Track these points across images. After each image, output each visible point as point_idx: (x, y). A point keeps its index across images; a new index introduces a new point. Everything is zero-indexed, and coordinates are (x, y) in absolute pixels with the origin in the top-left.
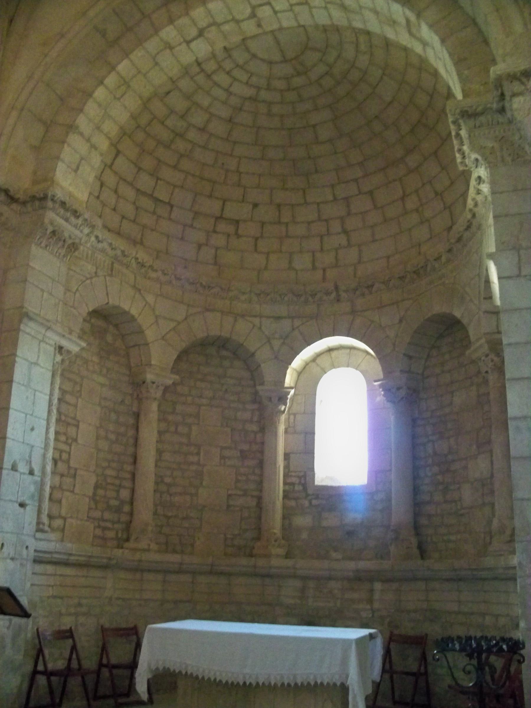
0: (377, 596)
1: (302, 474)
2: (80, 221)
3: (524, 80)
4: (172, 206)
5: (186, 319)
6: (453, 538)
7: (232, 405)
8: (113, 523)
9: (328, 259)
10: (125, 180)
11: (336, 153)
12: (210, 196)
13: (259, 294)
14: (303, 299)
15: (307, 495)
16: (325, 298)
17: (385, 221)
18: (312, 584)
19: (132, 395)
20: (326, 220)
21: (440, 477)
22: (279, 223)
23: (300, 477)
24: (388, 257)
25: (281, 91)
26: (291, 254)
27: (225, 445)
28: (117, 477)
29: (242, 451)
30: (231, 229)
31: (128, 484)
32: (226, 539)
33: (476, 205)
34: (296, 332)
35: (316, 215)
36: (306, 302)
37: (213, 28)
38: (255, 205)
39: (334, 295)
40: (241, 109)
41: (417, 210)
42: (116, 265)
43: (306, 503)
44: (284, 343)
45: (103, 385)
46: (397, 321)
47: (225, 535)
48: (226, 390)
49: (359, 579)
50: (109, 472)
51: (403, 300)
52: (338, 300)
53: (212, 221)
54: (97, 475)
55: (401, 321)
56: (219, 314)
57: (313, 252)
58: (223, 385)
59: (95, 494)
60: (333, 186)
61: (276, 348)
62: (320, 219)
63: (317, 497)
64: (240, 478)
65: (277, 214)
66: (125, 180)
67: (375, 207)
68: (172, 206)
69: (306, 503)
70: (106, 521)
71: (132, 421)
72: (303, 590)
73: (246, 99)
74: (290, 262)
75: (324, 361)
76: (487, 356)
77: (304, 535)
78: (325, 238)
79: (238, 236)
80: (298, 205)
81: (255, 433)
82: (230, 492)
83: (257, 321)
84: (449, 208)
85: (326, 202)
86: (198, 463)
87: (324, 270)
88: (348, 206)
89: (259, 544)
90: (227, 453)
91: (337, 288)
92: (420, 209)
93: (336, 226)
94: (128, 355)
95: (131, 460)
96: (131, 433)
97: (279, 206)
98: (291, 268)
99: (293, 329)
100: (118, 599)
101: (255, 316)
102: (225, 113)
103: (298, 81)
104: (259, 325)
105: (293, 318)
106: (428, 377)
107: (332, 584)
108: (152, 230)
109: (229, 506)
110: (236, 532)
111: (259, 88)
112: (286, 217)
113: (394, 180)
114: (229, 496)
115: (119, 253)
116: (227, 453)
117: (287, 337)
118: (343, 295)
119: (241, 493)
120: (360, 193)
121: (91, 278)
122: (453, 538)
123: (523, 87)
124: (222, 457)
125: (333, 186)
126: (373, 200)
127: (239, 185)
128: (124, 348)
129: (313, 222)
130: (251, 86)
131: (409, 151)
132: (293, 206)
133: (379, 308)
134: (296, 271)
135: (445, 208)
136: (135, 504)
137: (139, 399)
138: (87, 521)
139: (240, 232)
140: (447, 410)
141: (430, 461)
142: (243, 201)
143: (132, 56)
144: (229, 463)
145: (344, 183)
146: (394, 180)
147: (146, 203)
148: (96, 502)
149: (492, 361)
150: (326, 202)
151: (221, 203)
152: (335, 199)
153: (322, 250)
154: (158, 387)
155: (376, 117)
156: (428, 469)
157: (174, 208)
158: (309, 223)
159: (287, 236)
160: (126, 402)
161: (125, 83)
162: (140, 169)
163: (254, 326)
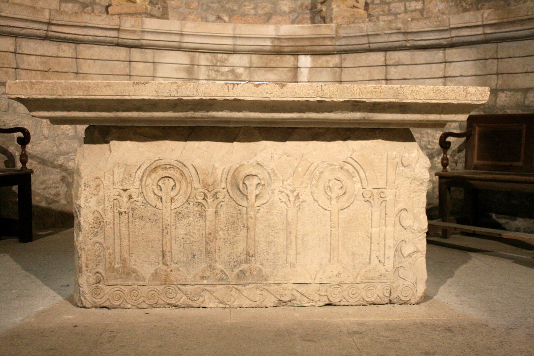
18: (203, 59)
49: (278, 52)
107: (235, 59)
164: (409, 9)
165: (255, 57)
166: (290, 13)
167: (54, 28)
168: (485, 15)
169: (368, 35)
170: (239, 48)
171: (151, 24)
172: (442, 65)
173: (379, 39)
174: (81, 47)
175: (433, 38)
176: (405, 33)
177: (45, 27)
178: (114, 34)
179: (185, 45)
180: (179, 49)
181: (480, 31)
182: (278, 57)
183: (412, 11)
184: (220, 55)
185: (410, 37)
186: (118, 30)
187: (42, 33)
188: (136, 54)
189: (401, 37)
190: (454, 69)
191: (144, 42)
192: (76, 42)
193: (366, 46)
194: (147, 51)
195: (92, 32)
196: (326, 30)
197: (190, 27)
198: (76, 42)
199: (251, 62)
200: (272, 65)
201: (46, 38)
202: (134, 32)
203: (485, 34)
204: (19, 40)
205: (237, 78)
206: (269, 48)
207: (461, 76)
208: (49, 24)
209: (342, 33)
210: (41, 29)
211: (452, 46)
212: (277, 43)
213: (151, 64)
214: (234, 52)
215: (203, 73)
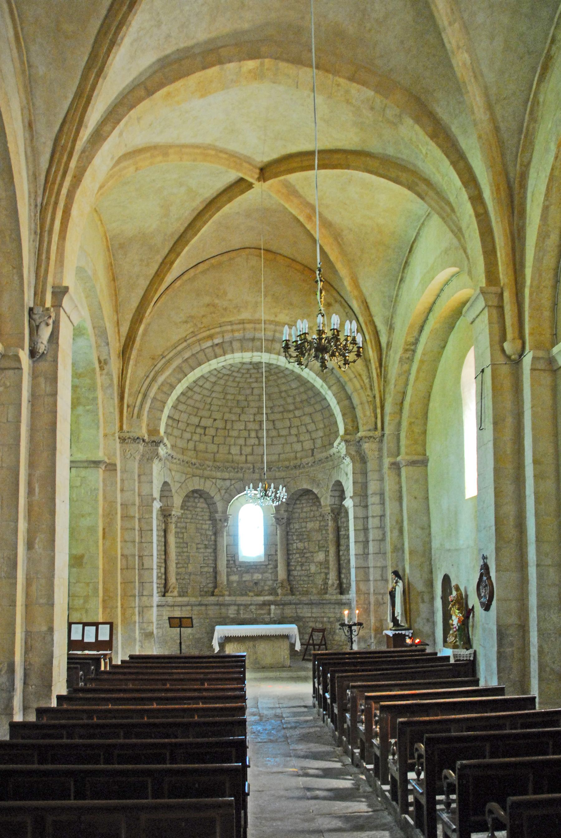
9: (248, 450)
20: (249, 430)
21: (300, 559)
22: (225, 429)
26: (230, 445)
30: (202, 431)
31: (163, 565)
34: (232, 487)
38: (215, 420)
41: (296, 435)
43: (235, 570)
52: (254, 472)
60: (255, 415)
62: (245, 429)
63: (240, 567)
67: (275, 428)
69: (235, 570)
77: (235, 585)
78: (247, 439)
83: (214, 481)
85: (250, 421)
87: (246, 456)
90: (199, 546)
93: (253, 434)
95: (163, 553)
96: (163, 540)
97: (226, 421)
98: (229, 453)
105: (231, 480)
109: (201, 572)
116: (199, 546)
118: (257, 471)
124: (197, 548)
126: (274, 425)
131: (296, 409)
132: (233, 421)
136: (168, 575)
137: (166, 523)
140: (304, 529)
150: (250, 421)
152: (254, 420)
153: (245, 445)
158: (240, 430)
159: (228, 436)
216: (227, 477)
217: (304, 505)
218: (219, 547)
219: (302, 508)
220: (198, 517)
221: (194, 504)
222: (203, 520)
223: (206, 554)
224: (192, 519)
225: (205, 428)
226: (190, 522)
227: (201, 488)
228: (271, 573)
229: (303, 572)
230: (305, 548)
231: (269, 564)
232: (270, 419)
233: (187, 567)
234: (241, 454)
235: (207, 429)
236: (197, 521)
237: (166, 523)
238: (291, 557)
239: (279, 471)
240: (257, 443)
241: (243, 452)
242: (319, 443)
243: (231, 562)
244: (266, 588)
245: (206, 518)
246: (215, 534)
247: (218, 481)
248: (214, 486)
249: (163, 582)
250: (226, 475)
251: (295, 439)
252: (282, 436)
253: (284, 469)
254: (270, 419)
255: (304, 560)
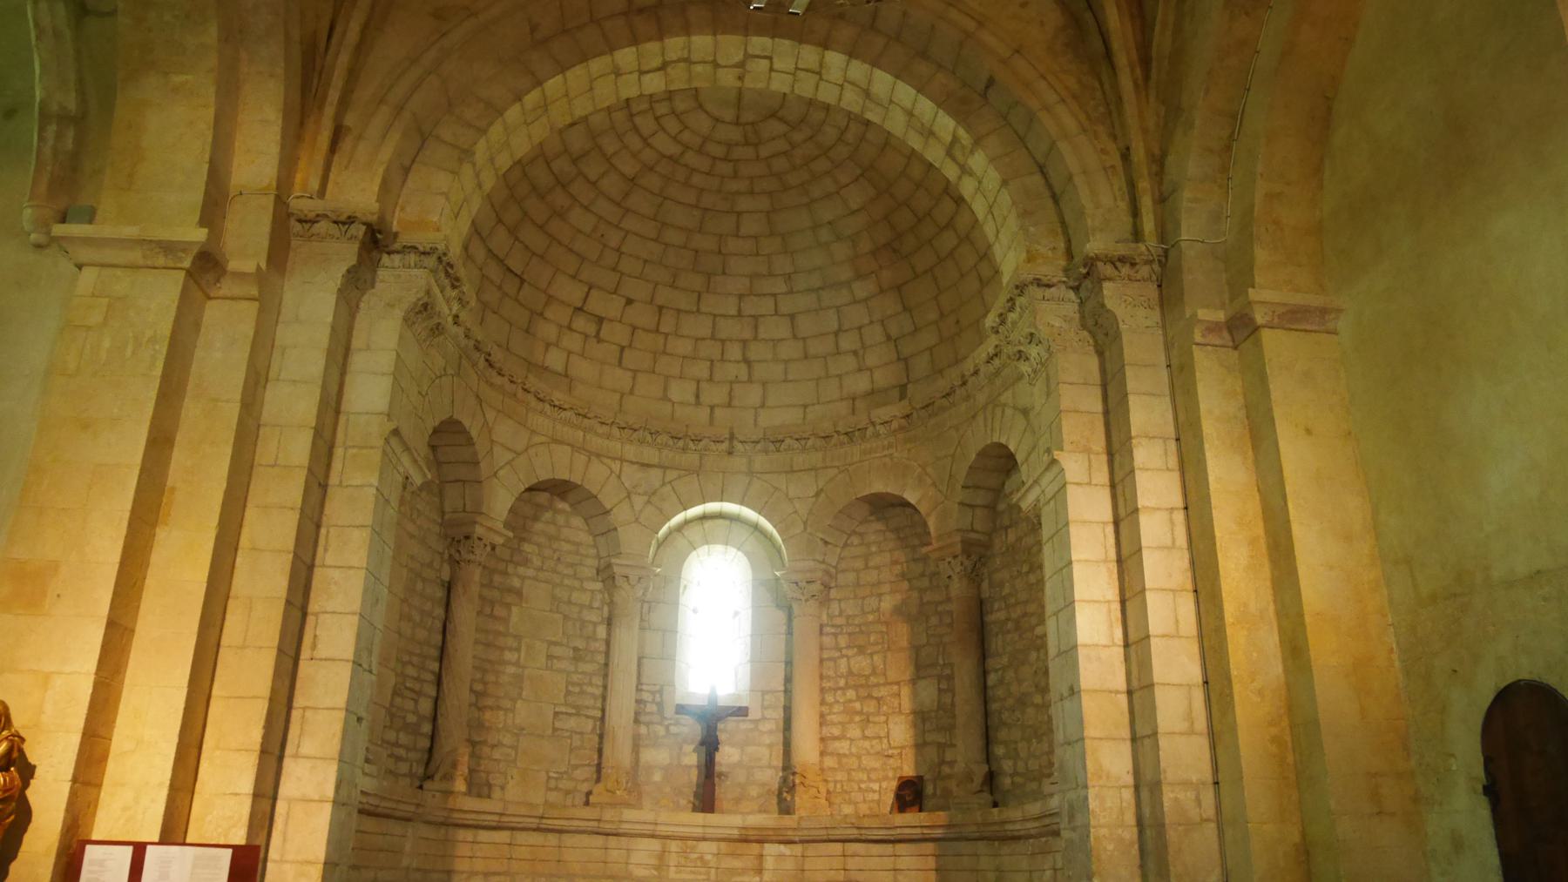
0: (769, 863)
1: (657, 688)
2: (454, 293)
3: (1118, 264)
4: (522, 281)
5: (526, 450)
6: (876, 786)
7: (566, 582)
8: (408, 749)
10: (479, 234)
11: (757, 254)
12: (574, 277)
13: (624, 428)
14: (681, 443)
15: (664, 718)
16: (713, 446)
17: (806, 357)
18: (674, 846)
19: (441, 554)
20: (723, 341)
21: (857, 706)
22: (657, 331)
23: (653, 693)
24: (805, 406)
25: (714, 158)
26: (667, 378)
27: (554, 639)
28: (417, 679)
29: (576, 649)
30: (591, 329)
31: (431, 690)
32: (549, 778)
33: (976, 373)
34: (668, 487)
35: (710, 331)
36: (684, 449)
37: (682, 65)
39: (725, 446)
40: (651, 169)
41: (855, 353)
42: (464, 361)
44: (649, 502)
45: (412, 536)
46: (812, 494)
47: (547, 772)
48: (559, 559)
49: (745, 840)
50: (411, 671)
51: (826, 467)
53: (570, 311)
54: (397, 675)
55: (817, 495)
56: (568, 449)
57: (698, 382)
58: (555, 551)
59: (392, 705)
60: (741, 297)
61: (637, 507)
62: (713, 338)
64: (570, 688)
65: (657, 318)
66: (479, 234)
67: (795, 337)
68: (522, 281)
69: (661, 730)
70: (401, 746)
71: (440, 593)
72: (662, 855)
73: (664, 156)
74: (666, 389)
75: (694, 533)
76: (955, 557)
77: (657, 777)
79: (599, 341)
80: (687, 312)
81: (595, 624)
82: (557, 710)
83: (616, 466)
84: (906, 360)
86: (517, 664)
87: (712, 408)
88: (756, 327)
89: (601, 786)
90: (557, 651)
91: (732, 437)
92: (861, 352)
93: (734, 352)
94: (441, 494)
95: (435, 653)
96: (439, 612)
97: (661, 308)
98: (665, 398)
99: (664, 484)
100: (418, 870)
101: (614, 459)
102: (629, 168)
103: (739, 153)
104: (618, 473)
106: (843, 571)
107: (705, 847)
108: (495, 313)
109: (555, 730)
110: (563, 769)
111: (687, 147)
112: (668, 325)
113: (829, 308)
114: (556, 714)
115: (472, 343)
116: (557, 651)
117: (654, 493)
118: (739, 447)
119: (574, 711)
120: (776, 313)
121: (441, 377)
122: (876, 786)
123: (1116, 273)
124: (550, 657)
125: (741, 297)
127: (614, 269)
128: (437, 482)
129: (703, 339)
130: (679, 142)
132: (679, 311)
133: (786, 472)
134: (673, 403)
135: (899, 359)
136: (440, 721)
137: (455, 563)
138: (381, 746)
139: (602, 335)
140: (871, 618)
141: (842, 683)
142: (615, 293)
143: (569, 74)
144: (557, 664)
145: (755, 295)
146: (829, 308)
147: (494, 271)
148: (392, 716)
149: (962, 564)
151: (586, 290)
152: (740, 314)
153: (711, 379)
154: (486, 545)
155: (830, 223)
156: (839, 692)
157: (526, 285)
158: (697, 339)
159: (664, 353)
160: (436, 565)
161: (544, 106)
162: (500, 221)
163: (612, 472)
164: (867, 799)
165: (723, 844)
166: (758, 797)
167: (544, 821)
168: (922, 817)
169: (826, 828)
170: (708, 836)
171: (629, 814)
172: (893, 858)
173: (838, 832)
174: (565, 837)
175: (882, 834)
176: (858, 828)
177: (537, 821)
178: (595, 824)
179: (658, 833)
180: (653, 836)
181: (918, 831)
182: (745, 845)
183: (870, 801)
184: (689, 842)
185: (863, 832)
186: (599, 821)
187: (534, 826)
188: (613, 841)
189: (855, 831)
190: (904, 863)
191: (621, 831)
192: (561, 832)
193: (825, 838)
194: (623, 838)
195: (576, 823)
196: (789, 821)
197: (664, 817)
198: (561, 832)
199: (719, 849)
200: (739, 852)
201: (538, 829)
202: (612, 822)
203: (923, 834)
204: (514, 832)
205: (705, 864)
206: (736, 837)
207: (909, 870)
208: (542, 818)
209: (804, 824)
210: (534, 822)
211: (900, 841)
212: (743, 832)
213: (625, 851)
214: (704, 839)
215: (673, 860)
216: (655, 461)
217: (874, 549)
218: (616, 658)
219: (866, 558)
220: (560, 568)
221: (552, 530)
222: (575, 576)
223: (575, 678)
224: (541, 569)
225: (600, 320)
226: (535, 579)
227: (576, 478)
228: (770, 746)
229: (867, 744)
230: (874, 672)
231: (764, 718)
232: (784, 309)
233: (513, 710)
234: (698, 402)
235: (605, 326)
236: (558, 581)
237: (455, 563)
238: (830, 698)
239: (804, 449)
240: (744, 375)
241: (704, 398)
242: (921, 365)
243: (651, 708)
244: (754, 791)
245: (588, 572)
246: (609, 622)
247: (627, 469)
248: (613, 478)
249: (426, 743)
250: (650, 454)
251: (850, 362)
252: (816, 357)
253: (819, 443)
254: (784, 309)
255: (870, 707)
